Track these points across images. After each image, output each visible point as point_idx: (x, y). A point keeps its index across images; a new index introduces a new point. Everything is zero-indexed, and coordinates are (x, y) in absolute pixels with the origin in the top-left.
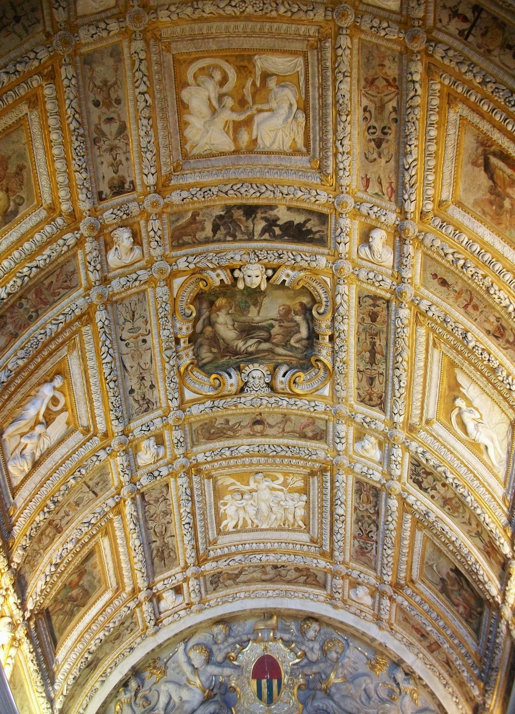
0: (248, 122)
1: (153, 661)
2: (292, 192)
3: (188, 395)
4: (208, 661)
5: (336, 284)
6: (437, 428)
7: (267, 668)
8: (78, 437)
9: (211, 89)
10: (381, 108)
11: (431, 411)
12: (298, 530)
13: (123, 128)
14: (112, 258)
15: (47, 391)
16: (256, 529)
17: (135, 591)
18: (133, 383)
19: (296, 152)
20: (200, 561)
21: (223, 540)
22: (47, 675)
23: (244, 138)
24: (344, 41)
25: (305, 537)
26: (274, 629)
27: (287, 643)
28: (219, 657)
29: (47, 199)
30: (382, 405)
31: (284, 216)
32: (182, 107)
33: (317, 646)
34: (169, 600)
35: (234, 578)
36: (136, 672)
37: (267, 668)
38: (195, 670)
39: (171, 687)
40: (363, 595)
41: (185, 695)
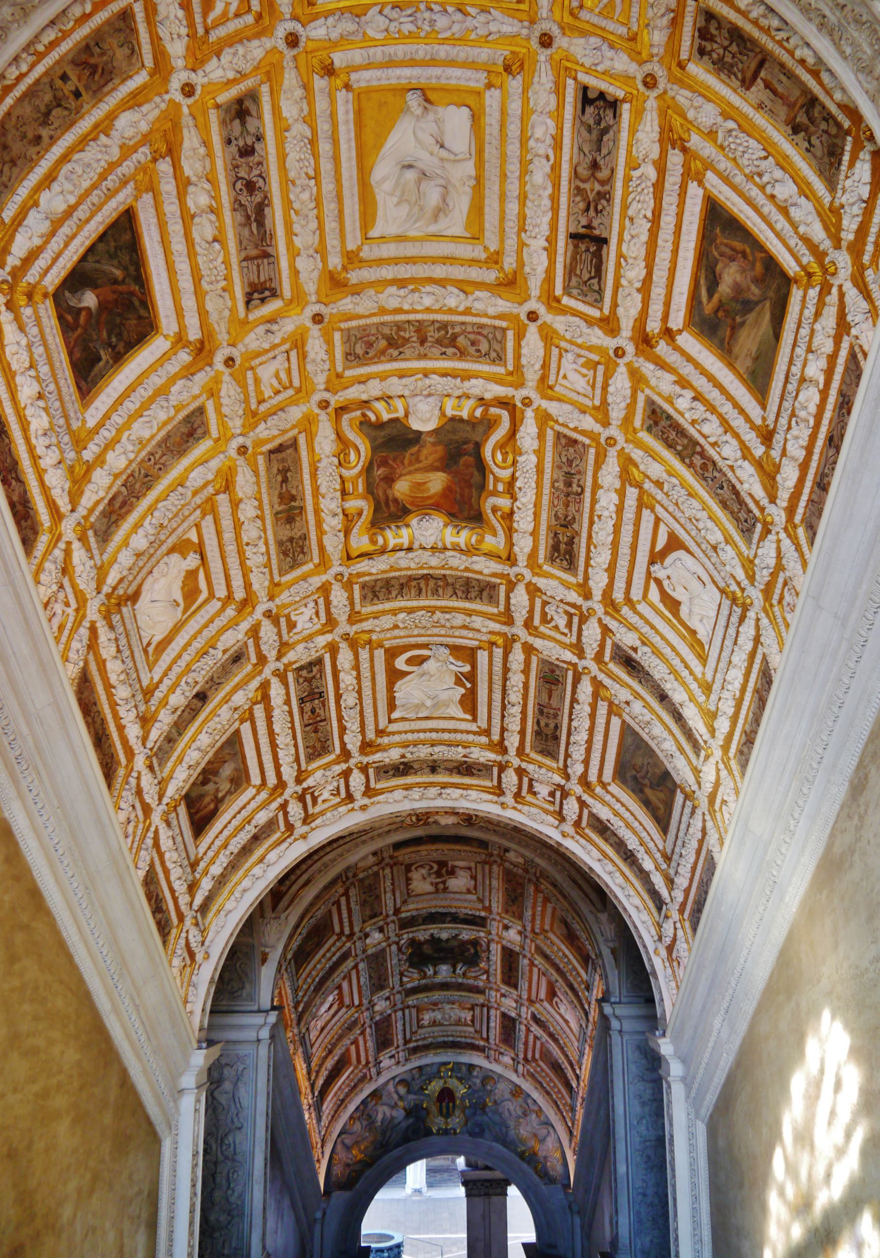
0: (444, 882)
1: (375, 1095)
2: (468, 906)
3: (405, 979)
4: (409, 1092)
5: (489, 942)
6: (546, 1004)
7: (446, 1095)
8: (344, 1010)
9: (424, 871)
10: (514, 890)
11: (543, 995)
12: (466, 1025)
13: (378, 897)
14: (368, 941)
15: (331, 998)
16: (442, 1025)
17: (368, 1063)
18: (375, 981)
19: (469, 891)
20: (406, 1042)
21: (420, 1031)
22: (319, 1119)
23: (441, 886)
24: (495, 868)
25: (471, 1029)
26: (452, 1070)
27: (460, 1079)
28: (417, 1088)
29: (337, 929)
30: (515, 987)
31: (462, 916)
32: (408, 880)
33: (478, 1081)
34: (386, 1063)
35: (427, 1048)
36: (363, 1102)
37: (446, 1095)
38: (401, 1098)
39: (386, 1109)
40: (507, 1059)
41: (395, 1113)
